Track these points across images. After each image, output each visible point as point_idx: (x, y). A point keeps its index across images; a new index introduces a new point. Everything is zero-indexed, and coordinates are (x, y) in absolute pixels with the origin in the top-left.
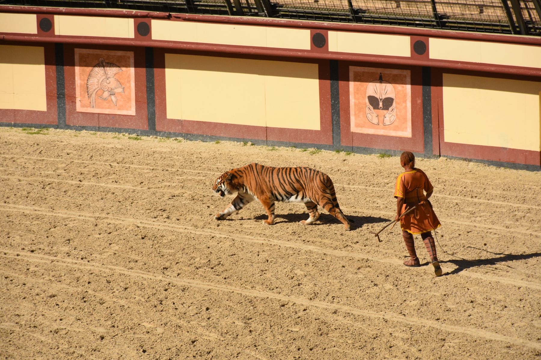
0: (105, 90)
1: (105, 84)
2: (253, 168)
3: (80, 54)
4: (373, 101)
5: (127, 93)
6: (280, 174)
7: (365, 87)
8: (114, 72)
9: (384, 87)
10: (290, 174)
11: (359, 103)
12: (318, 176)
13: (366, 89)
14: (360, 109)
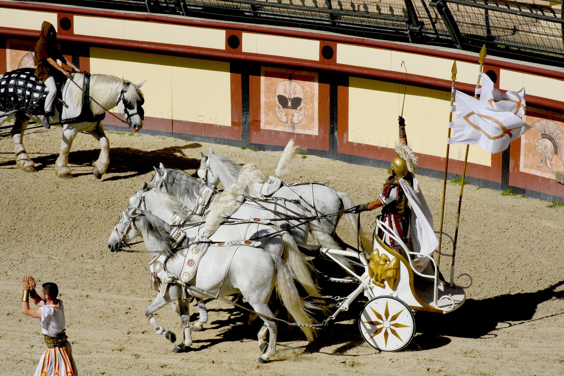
4: (283, 100)
7: (275, 86)
9: (293, 88)
14: (270, 107)
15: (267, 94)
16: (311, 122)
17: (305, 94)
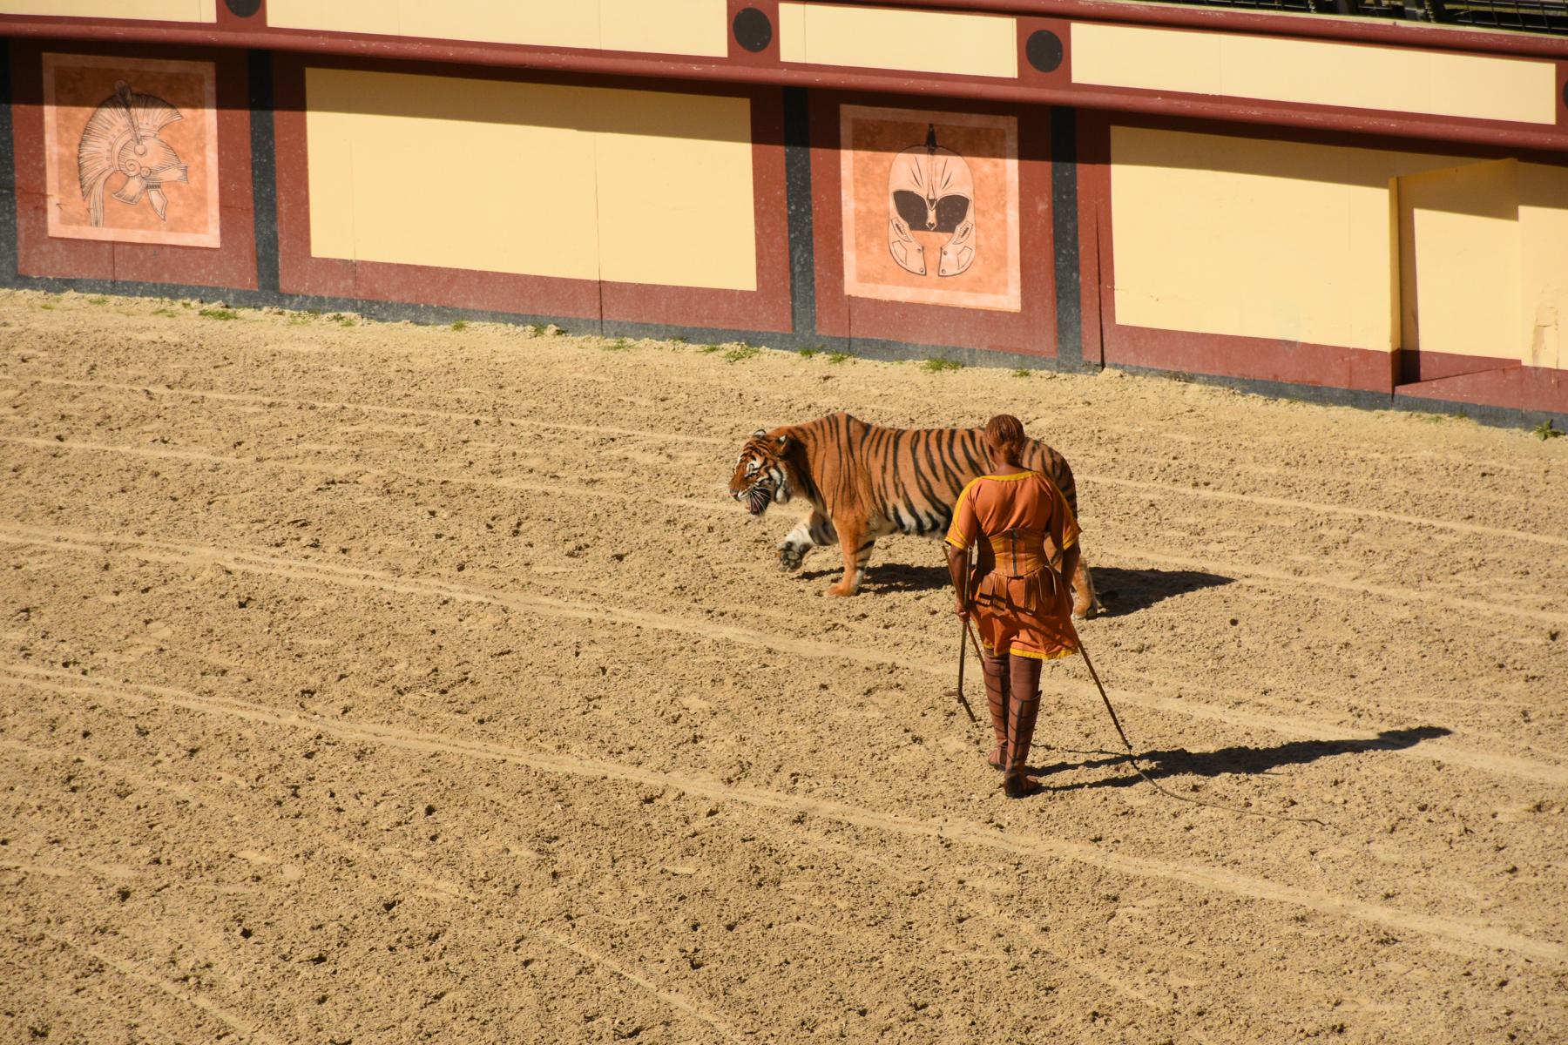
0: (132, 174)
1: (132, 156)
2: (837, 427)
3: (856, 122)
4: (910, 206)
5: (194, 181)
6: (921, 448)
7: (886, 164)
8: (158, 123)
9: (941, 166)
10: (950, 447)
11: (870, 211)
12: (1038, 453)
13: (888, 171)
14: (871, 228)
15: (862, 190)
16: (998, 270)
17: (979, 184)
